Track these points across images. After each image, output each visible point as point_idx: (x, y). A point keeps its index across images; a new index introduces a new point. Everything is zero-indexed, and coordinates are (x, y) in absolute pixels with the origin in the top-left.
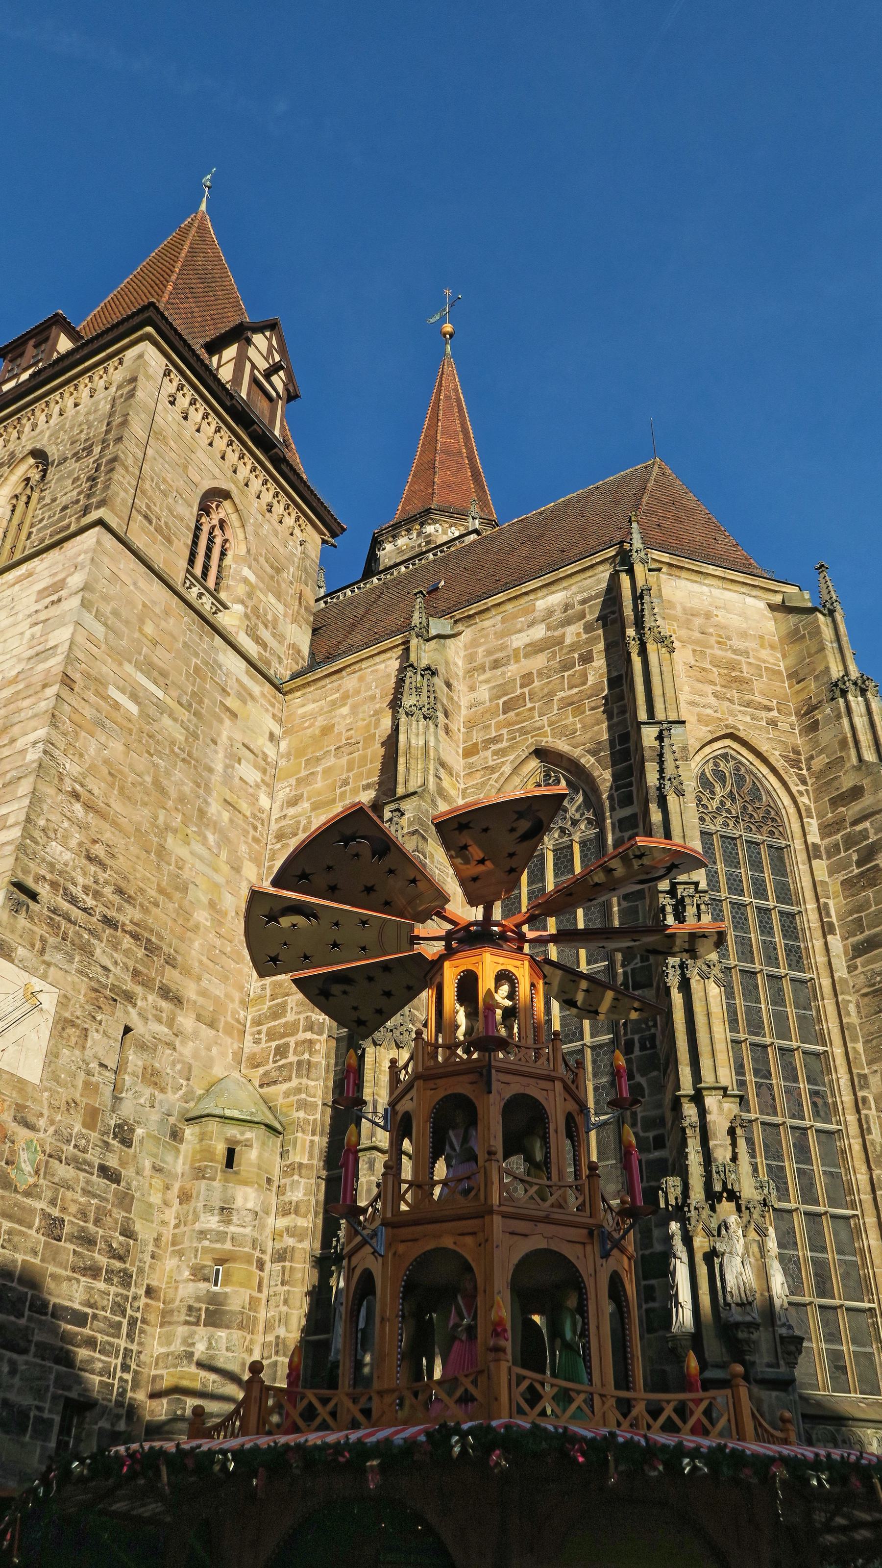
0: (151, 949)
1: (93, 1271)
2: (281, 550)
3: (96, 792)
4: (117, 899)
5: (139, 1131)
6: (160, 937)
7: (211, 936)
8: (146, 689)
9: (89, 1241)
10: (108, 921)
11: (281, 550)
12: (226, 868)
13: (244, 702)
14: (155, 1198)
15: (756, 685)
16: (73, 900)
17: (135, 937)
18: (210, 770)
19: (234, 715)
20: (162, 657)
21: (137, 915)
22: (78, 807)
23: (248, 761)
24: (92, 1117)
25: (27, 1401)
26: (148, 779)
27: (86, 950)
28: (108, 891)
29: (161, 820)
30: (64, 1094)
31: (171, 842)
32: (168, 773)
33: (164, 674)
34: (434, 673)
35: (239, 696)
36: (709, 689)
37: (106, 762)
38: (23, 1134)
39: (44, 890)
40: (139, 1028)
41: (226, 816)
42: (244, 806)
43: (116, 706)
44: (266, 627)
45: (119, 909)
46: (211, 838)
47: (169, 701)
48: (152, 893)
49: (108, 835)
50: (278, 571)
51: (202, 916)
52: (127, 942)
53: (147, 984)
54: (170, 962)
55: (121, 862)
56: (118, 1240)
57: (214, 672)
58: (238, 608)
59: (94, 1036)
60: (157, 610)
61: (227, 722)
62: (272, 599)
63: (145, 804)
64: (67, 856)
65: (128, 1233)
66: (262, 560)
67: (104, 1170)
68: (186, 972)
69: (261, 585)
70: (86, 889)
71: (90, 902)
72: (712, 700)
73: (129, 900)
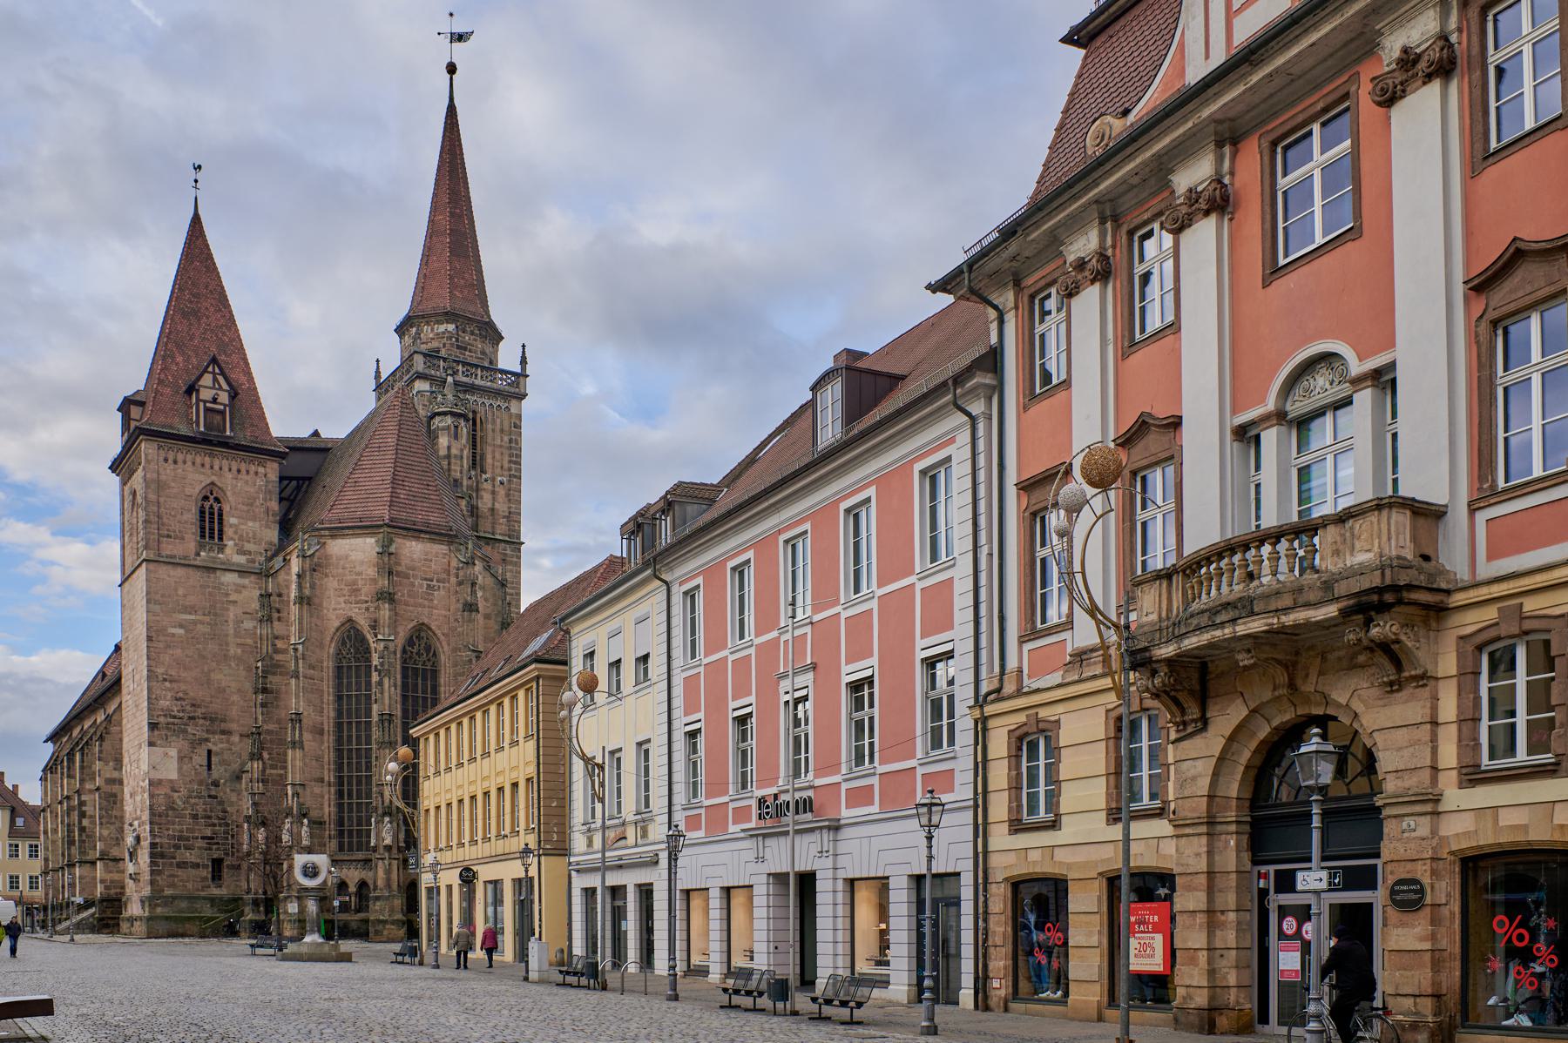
0: (212, 720)
1: (214, 825)
2: (252, 490)
3: (173, 673)
4: (192, 709)
5: (222, 781)
6: (217, 714)
7: (242, 703)
8: (185, 620)
9: (210, 817)
10: (190, 718)
11: (252, 490)
12: (244, 673)
13: (240, 592)
14: (234, 798)
15: (363, 591)
16: (174, 717)
17: (205, 718)
18: (227, 635)
19: (235, 602)
20: (191, 600)
21: (203, 711)
22: (167, 684)
23: (247, 619)
24: (200, 783)
25: (198, 861)
26: (196, 656)
27: (185, 731)
28: (188, 708)
29: (206, 669)
30: (188, 779)
31: (212, 675)
32: (205, 649)
33: (193, 607)
34: (270, 595)
35: (236, 591)
36: (342, 599)
37: (174, 660)
38: (176, 794)
39: (162, 719)
40: (214, 748)
41: (239, 651)
42: (249, 641)
43: (173, 635)
44: (249, 542)
45: (195, 711)
46: (233, 664)
47: (198, 617)
48: (208, 699)
49: (183, 687)
50: (252, 505)
51: (235, 698)
52: (201, 722)
53: (214, 733)
54: (224, 721)
55: (191, 694)
56: (220, 815)
57: (220, 589)
58: (231, 543)
59: (195, 757)
60: (183, 580)
61: (232, 607)
62: (250, 524)
63: (196, 667)
64: (168, 703)
65: (225, 811)
66: (240, 506)
67: (210, 796)
68: (232, 721)
69: (242, 521)
70: (178, 711)
71: (181, 715)
72: (343, 605)
73: (199, 706)
